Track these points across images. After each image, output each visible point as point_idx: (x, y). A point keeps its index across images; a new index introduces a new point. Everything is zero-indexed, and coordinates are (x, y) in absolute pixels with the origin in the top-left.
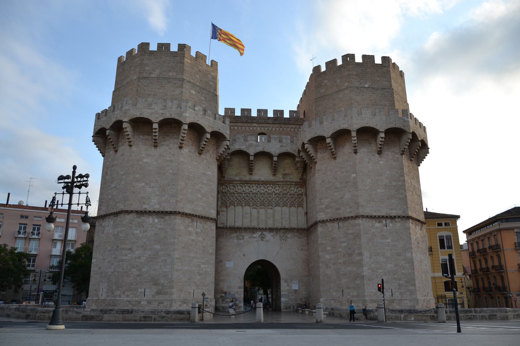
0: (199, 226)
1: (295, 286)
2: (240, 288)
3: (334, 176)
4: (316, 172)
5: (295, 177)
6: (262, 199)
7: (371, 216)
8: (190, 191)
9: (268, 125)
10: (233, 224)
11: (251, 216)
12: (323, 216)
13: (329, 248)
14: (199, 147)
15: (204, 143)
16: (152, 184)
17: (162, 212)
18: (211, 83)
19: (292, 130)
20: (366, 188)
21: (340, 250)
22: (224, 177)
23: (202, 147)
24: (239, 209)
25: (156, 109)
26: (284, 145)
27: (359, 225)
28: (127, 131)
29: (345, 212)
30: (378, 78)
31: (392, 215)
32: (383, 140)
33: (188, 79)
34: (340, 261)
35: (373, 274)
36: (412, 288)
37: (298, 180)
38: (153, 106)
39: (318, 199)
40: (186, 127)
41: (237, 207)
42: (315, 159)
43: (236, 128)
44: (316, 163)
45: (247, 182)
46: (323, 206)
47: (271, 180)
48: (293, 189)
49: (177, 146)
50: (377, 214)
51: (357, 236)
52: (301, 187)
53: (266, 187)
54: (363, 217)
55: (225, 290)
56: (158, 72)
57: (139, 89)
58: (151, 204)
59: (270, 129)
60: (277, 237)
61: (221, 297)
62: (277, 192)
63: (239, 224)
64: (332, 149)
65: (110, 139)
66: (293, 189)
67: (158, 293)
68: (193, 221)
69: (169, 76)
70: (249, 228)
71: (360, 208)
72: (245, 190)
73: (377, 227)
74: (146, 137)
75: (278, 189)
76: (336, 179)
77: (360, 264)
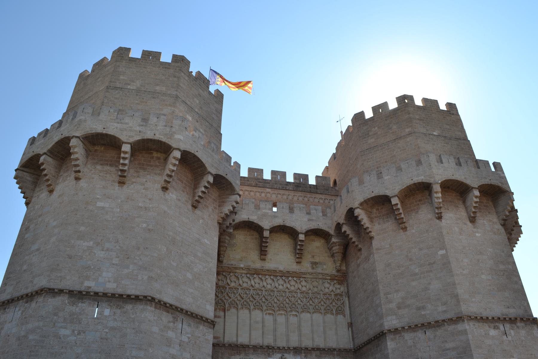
0: (187, 330)
4: (375, 251)
5: (329, 267)
6: (281, 299)
8: (175, 264)
9: (287, 192)
10: (234, 339)
11: (263, 326)
12: (394, 322)
14: (194, 196)
15: (203, 189)
16: (107, 245)
17: (121, 296)
18: (214, 116)
19: (321, 201)
20: (464, 272)
23: (199, 196)
24: (244, 314)
25: (131, 124)
26: (314, 218)
27: (465, 332)
28: (76, 153)
29: (434, 312)
30: (448, 127)
31: (512, 316)
32: (478, 200)
33: (183, 99)
37: (334, 272)
38: (127, 120)
39: (382, 295)
40: (178, 154)
41: (241, 312)
42: (370, 232)
44: (371, 238)
45: (257, 272)
46: (393, 305)
49: (159, 186)
52: (339, 284)
57: (106, 101)
58: (101, 280)
59: (290, 197)
62: (304, 289)
63: (243, 339)
65: (46, 175)
66: (327, 285)
68: (175, 320)
70: (262, 347)
71: (461, 303)
72: (253, 284)
74: (108, 168)
76: (411, 260)
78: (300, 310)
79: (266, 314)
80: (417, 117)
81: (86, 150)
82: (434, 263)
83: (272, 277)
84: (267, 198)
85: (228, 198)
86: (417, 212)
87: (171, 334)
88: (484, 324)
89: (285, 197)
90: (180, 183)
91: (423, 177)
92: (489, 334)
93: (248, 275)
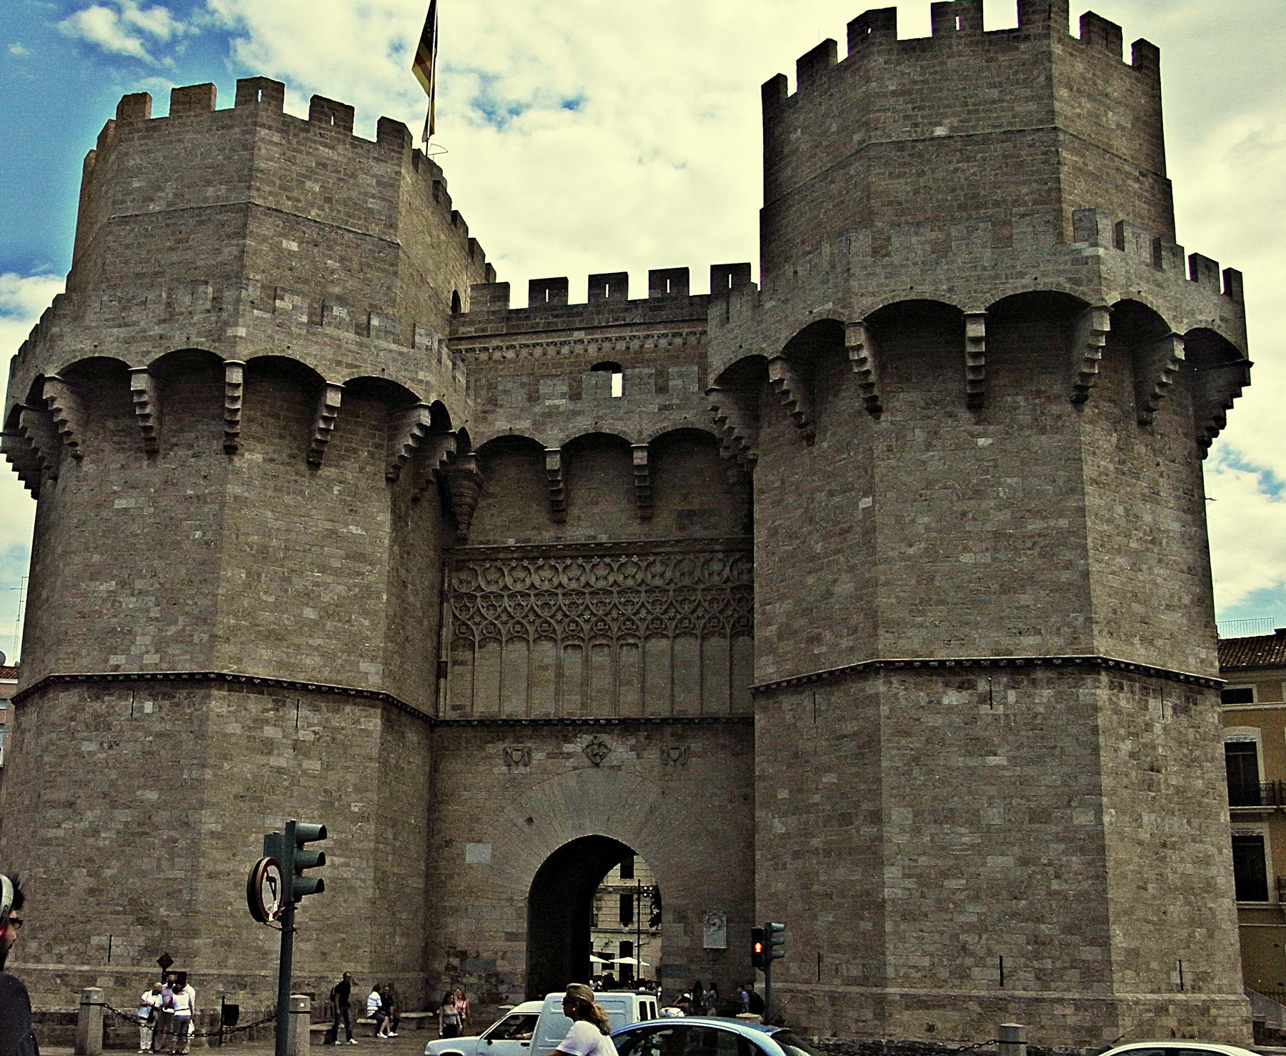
1: (715, 938)
2: (511, 937)
3: (807, 510)
7: (925, 664)
8: (271, 599)
9: (627, 333)
10: (495, 708)
11: (559, 675)
13: (783, 794)
20: (911, 551)
21: (817, 798)
22: (464, 540)
23: (317, 440)
24: (516, 652)
26: (676, 401)
27: (875, 700)
29: (838, 651)
34: (815, 842)
35: (923, 896)
36: (1088, 953)
41: (511, 647)
42: (746, 448)
43: (510, 354)
44: (754, 462)
47: (633, 539)
48: (716, 566)
49: (217, 445)
51: (870, 744)
53: (615, 566)
54: (891, 667)
55: (462, 943)
56: (170, 189)
59: (635, 345)
60: (653, 755)
61: (449, 968)
62: (658, 582)
63: (514, 707)
64: (793, 403)
69: (206, 200)
70: (548, 722)
71: (881, 631)
72: (536, 579)
73: (950, 709)
75: (660, 573)
77: (873, 857)
78: (641, 633)
81: (77, 393)
82: (849, 530)
83: (580, 561)
84: (578, 355)
87: (269, 731)
88: (934, 678)
89: (621, 346)
90: (271, 421)
92: (939, 703)
93: (525, 563)
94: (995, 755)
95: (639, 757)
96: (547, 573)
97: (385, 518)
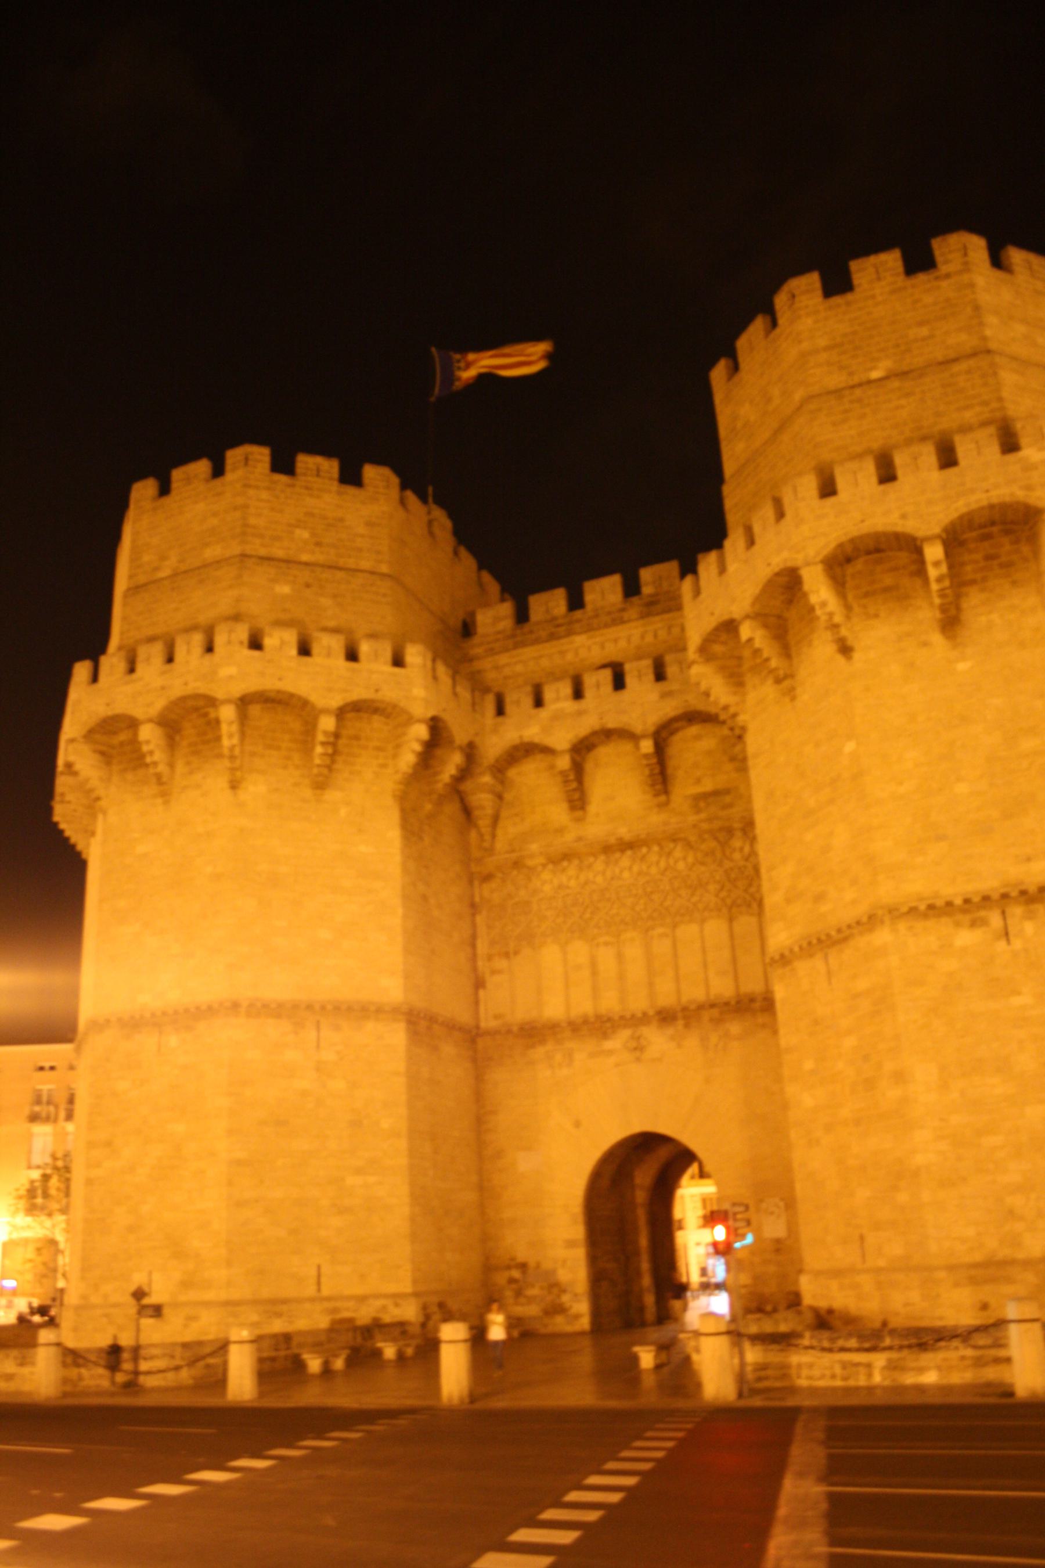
2: (570, 1244)
7: (931, 907)
11: (594, 973)
13: (809, 1065)
29: (843, 905)
30: (924, 331)
33: (263, 552)
40: (227, 713)
50: (954, 890)
55: (522, 1254)
61: (512, 1281)
63: (554, 1009)
64: (767, 660)
67: (186, 1284)
70: (586, 1021)
79: (598, 945)
80: (822, 342)
85: (404, 734)
86: (810, 644)
89: (622, 644)
91: (785, 554)
94: (1019, 993)
95: (679, 1046)
96: (572, 871)
97: (394, 835)
